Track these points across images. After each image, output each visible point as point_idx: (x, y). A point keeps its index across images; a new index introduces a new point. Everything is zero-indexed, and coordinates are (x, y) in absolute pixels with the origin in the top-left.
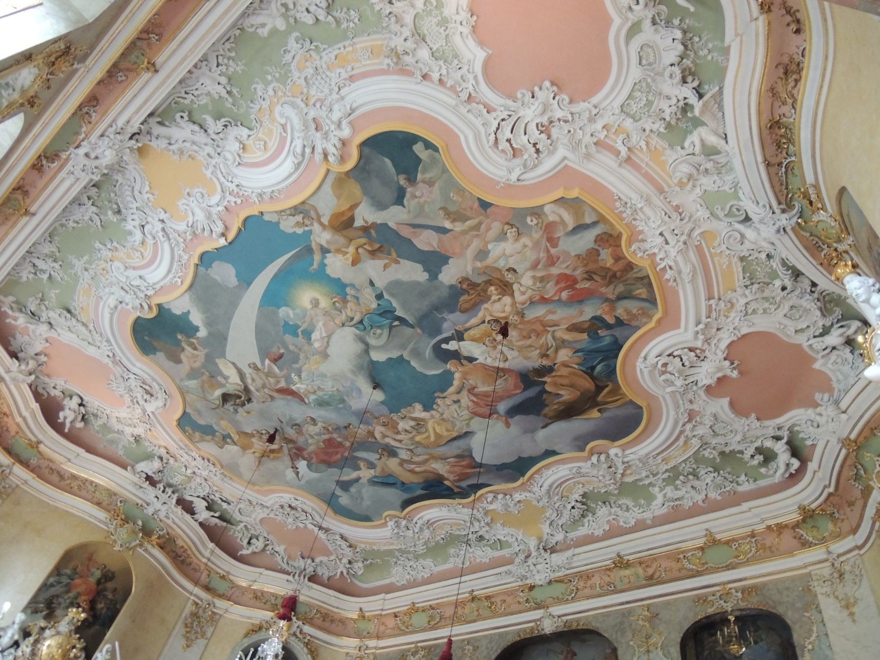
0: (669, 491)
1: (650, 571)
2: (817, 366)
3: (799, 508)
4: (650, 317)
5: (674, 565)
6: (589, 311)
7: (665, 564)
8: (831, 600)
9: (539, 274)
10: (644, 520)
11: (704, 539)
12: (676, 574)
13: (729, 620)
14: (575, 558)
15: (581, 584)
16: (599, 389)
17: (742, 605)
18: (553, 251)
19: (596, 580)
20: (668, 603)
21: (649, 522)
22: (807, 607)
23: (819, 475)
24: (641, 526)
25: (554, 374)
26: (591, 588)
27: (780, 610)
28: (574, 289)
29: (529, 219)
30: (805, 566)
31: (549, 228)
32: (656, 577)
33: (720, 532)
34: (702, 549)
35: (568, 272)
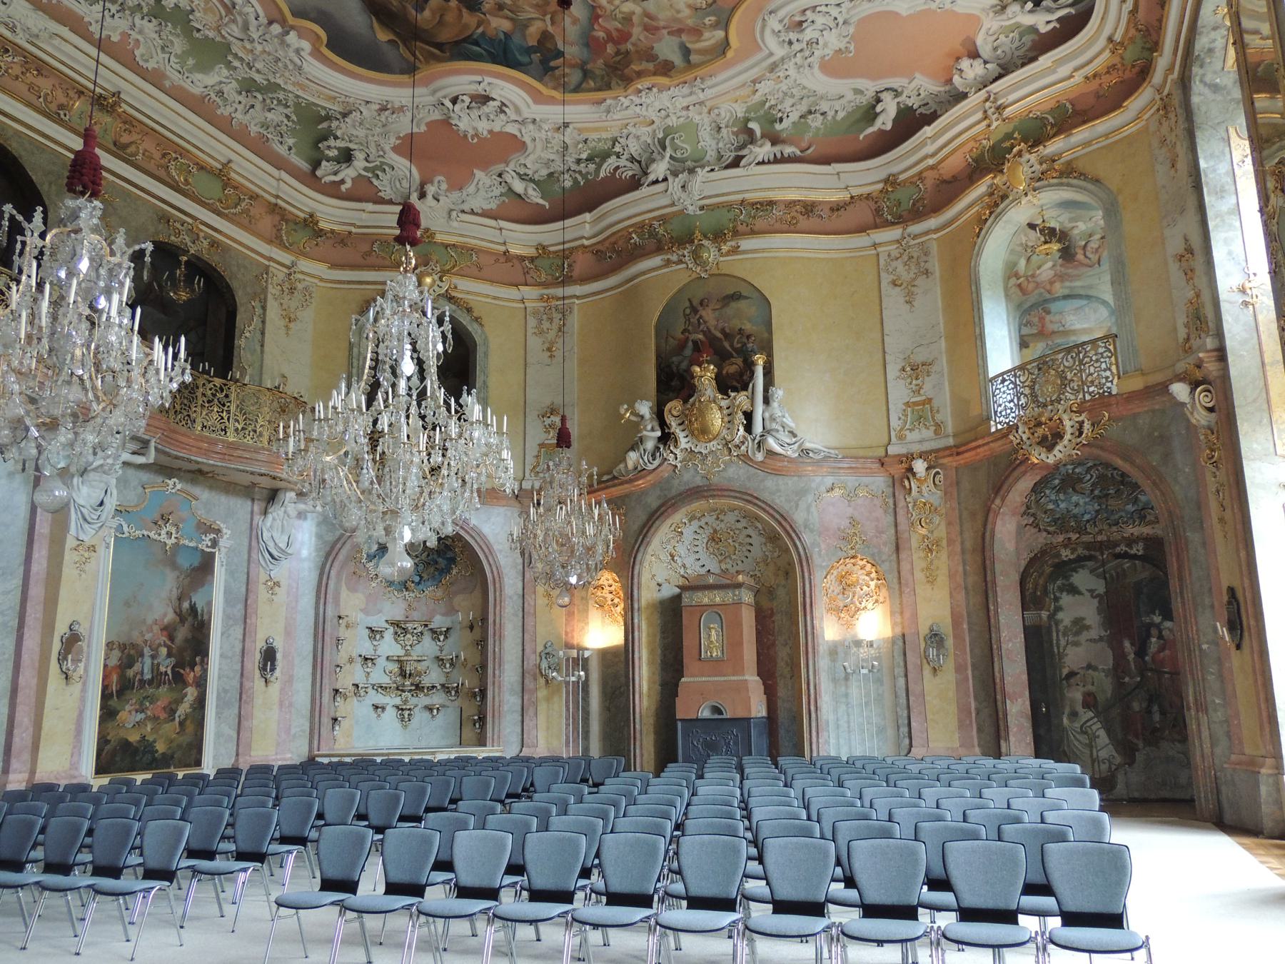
0: (230, 89)
1: (125, 139)
2: (479, 174)
3: (311, 216)
4: (555, 88)
5: (157, 155)
6: (573, 51)
7: (148, 145)
8: (276, 304)
9: (635, 19)
10: (163, 76)
11: (220, 167)
12: (151, 167)
13: (180, 262)
14: (57, 41)
15: (17, 70)
16: (440, 46)
17: (206, 257)
18: (665, 32)
19: (45, 84)
20: (130, 194)
21: (167, 84)
22: (254, 296)
23: (364, 215)
24: (155, 79)
25: (464, 10)
26: (31, 87)
27: (234, 284)
28: (606, 42)
29: (713, 18)
30: (270, 259)
31: (697, 32)
32: (128, 151)
33: (238, 174)
34: (202, 168)
35: (633, 39)
